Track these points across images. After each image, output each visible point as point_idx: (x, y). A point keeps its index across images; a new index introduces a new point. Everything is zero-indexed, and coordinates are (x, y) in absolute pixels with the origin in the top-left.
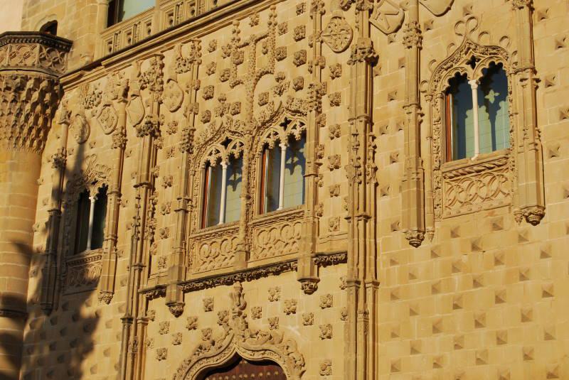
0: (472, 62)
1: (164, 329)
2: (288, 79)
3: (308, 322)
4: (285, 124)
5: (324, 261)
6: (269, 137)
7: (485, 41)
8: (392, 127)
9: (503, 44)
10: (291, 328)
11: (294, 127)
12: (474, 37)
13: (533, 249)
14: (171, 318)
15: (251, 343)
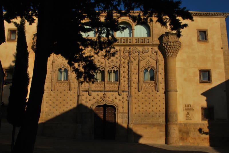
0: (149, 67)
1: (86, 98)
2: (114, 61)
3: (119, 100)
4: (113, 68)
5: (123, 92)
6: (109, 69)
7: (151, 65)
8: (135, 73)
9: (154, 67)
10: (117, 101)
11: (115, 69)
12: (150, 64)
13: (158, 95)
14: (88, 96)
15: (110, 102)
